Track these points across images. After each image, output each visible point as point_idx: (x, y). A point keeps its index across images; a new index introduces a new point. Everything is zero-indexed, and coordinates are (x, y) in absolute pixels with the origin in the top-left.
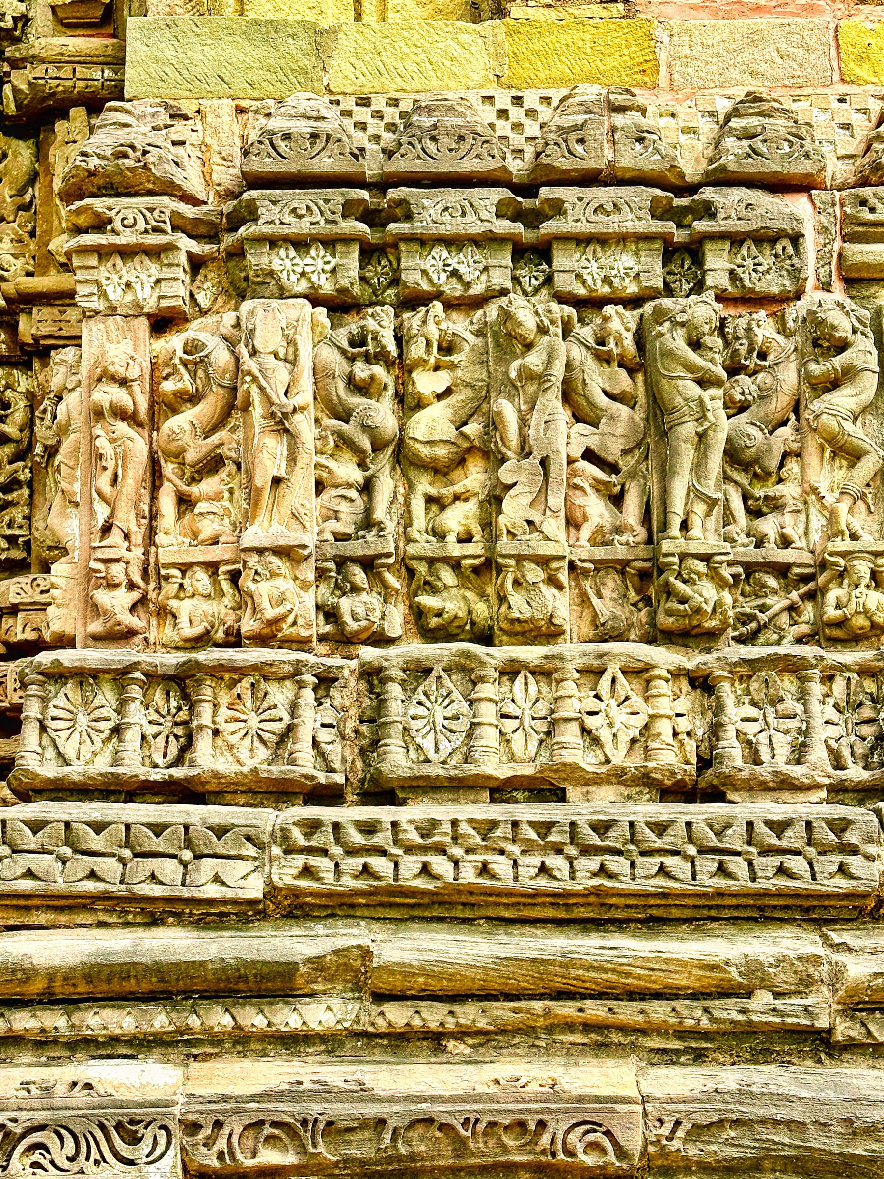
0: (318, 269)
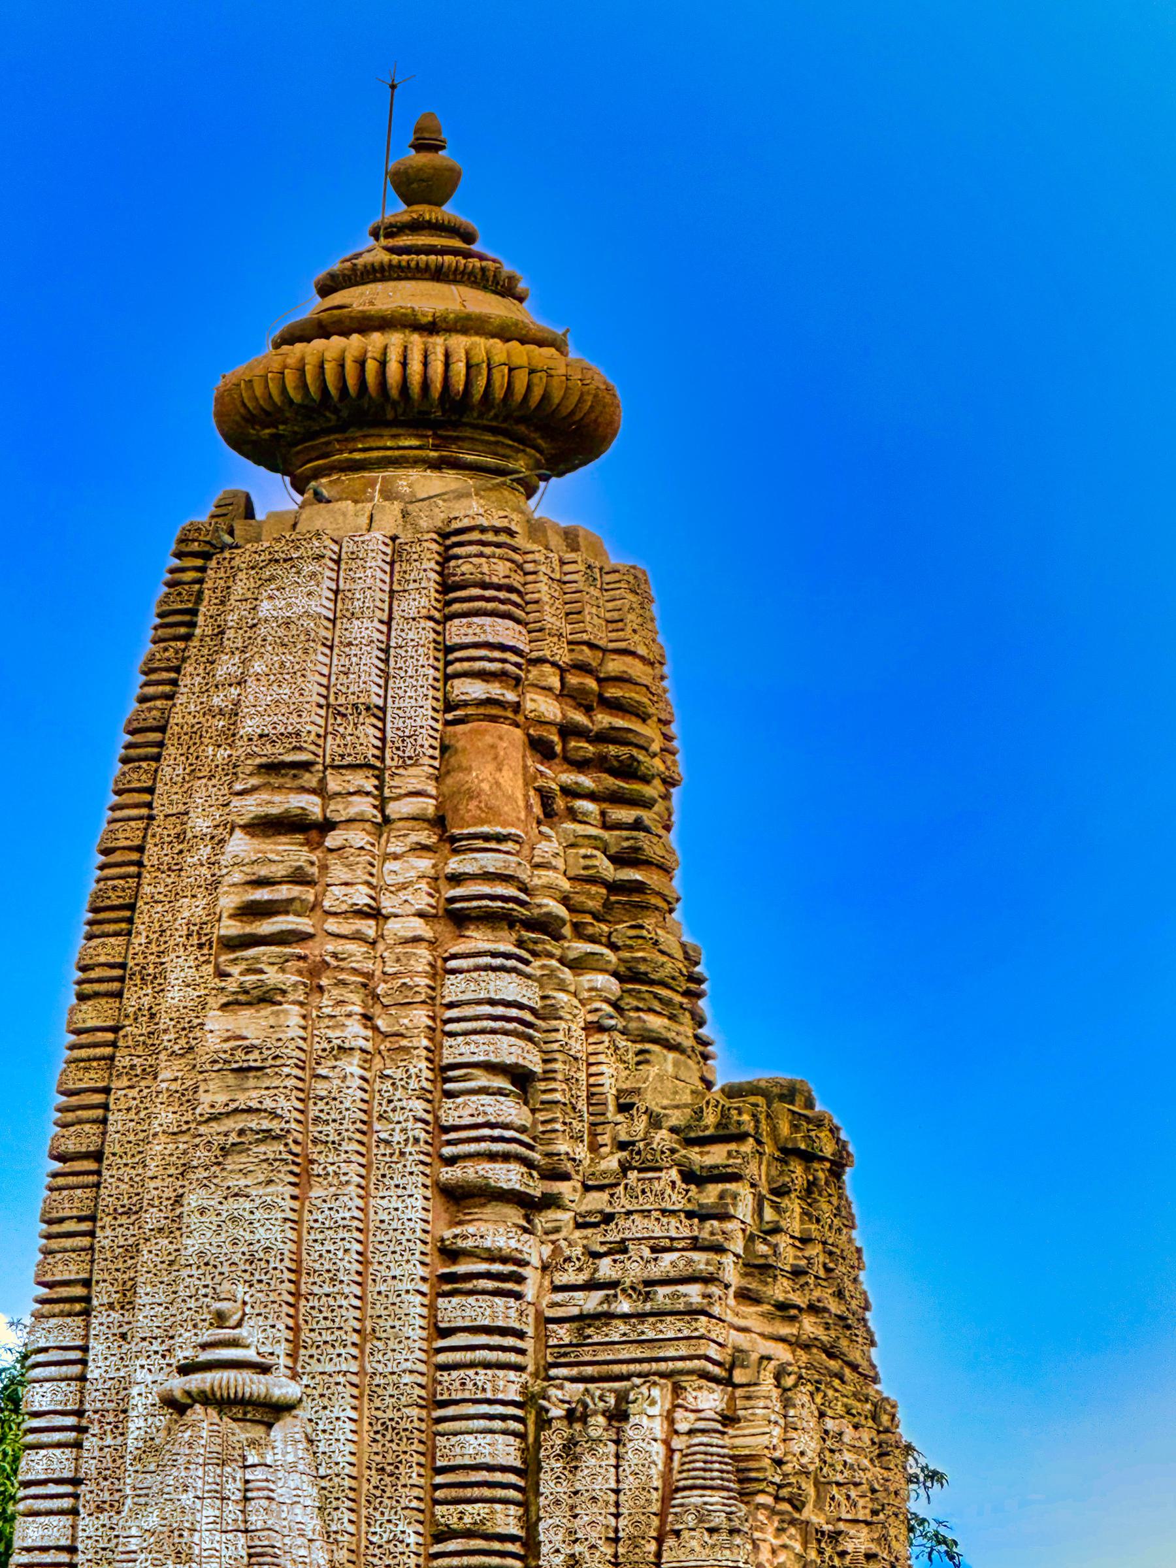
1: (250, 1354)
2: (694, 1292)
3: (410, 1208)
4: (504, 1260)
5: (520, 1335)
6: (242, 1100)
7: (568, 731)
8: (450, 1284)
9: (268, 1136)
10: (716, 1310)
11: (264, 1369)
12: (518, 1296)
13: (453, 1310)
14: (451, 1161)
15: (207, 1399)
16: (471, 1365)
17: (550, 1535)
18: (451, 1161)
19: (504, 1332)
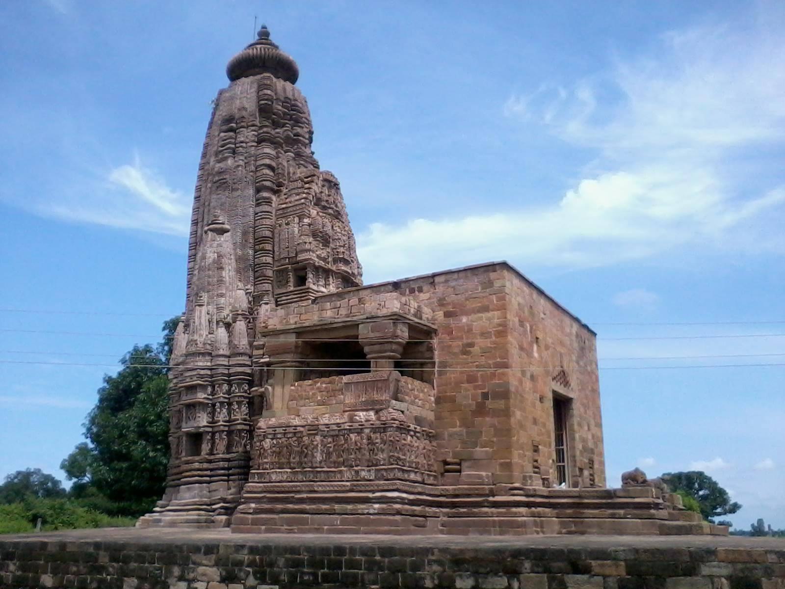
0: (270, 436)
1: (221, 222)
2: (303, 201)
3: (251, 191)
4: (268, 199)
5: (272, 213)
6: (220, 178)
7: (285, 113)
8: (258, 205)
9: (225, 183)
10: (307, 204)
11: (223, 224)
12: (271, 206)
13: (258, 209)
14: (257, 183)
15: (211, 230)
16: (261, 219)
17: (276, 249)
18: (257, 183)
19: (268, 212)
